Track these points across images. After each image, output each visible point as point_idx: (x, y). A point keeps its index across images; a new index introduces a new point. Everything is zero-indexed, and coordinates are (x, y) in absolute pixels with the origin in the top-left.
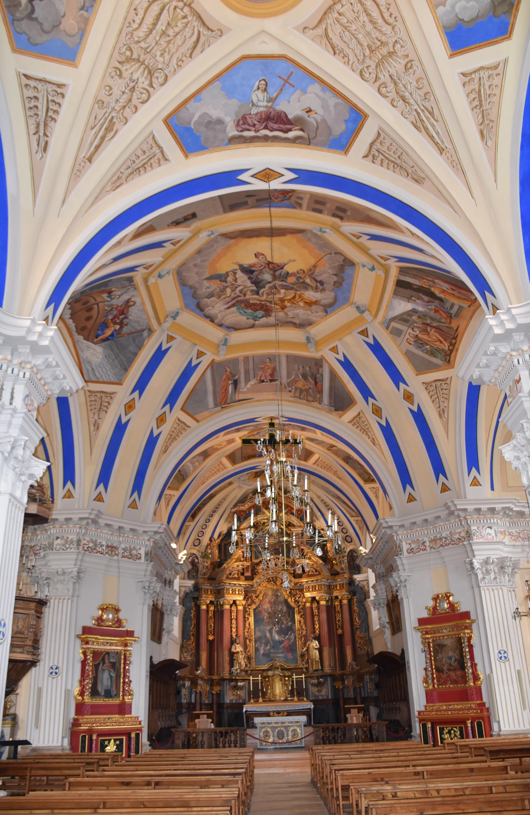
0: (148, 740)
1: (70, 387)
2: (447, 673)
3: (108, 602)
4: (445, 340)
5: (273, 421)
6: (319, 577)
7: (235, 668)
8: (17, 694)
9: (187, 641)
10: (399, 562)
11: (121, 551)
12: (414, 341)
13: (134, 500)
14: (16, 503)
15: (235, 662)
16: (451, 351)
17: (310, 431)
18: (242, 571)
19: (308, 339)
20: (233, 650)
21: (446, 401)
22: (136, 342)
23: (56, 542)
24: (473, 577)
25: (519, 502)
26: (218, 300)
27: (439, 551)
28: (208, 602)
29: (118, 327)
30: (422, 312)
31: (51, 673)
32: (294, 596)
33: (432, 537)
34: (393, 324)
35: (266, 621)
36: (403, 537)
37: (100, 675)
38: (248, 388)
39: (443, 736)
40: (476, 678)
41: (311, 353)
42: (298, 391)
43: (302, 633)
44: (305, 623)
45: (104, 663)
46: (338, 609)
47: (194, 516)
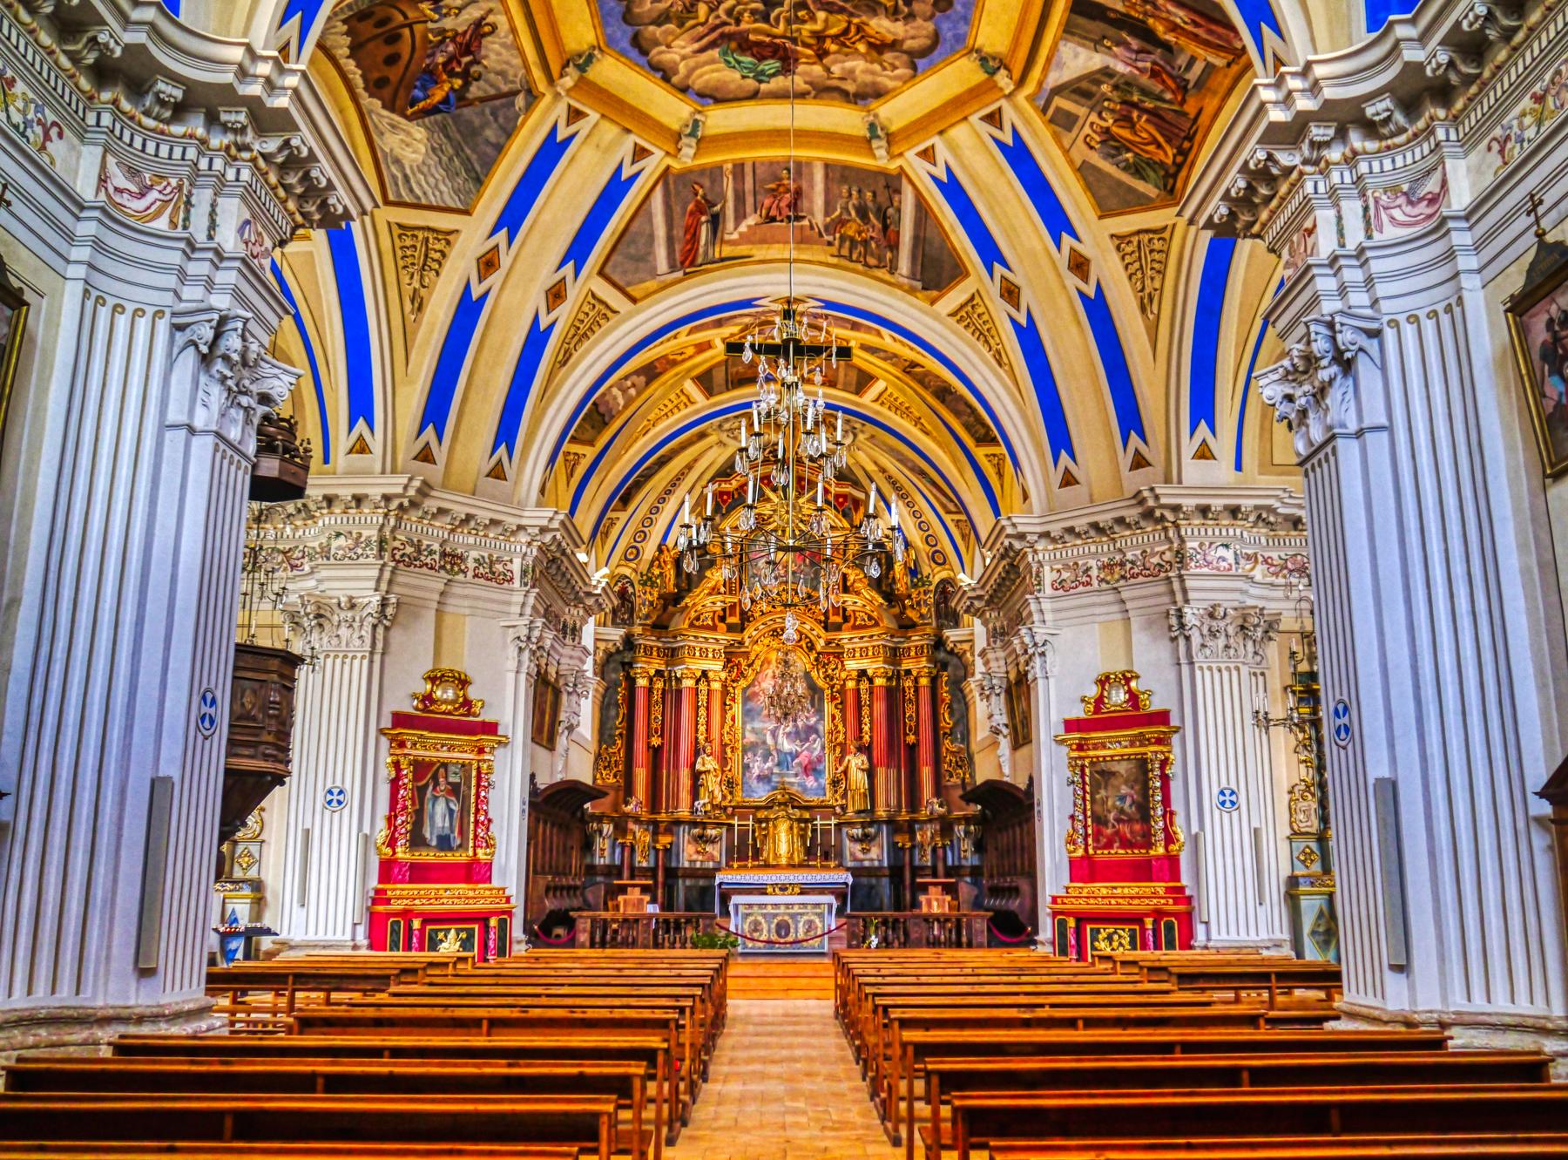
0: (525, 931)
1: (345, 208)
2: (1114, 826)
3: (446, 665)
4: (1169, 141)
5: (794, 307)
6: (875, 631)
7: (702, 802)
8: (263, 842)
9: (609, 746)
10: (1033, 607)
11: (471, 564)
12: (1102, 142)
13: (500, 461)
14: (229, 452)
15: (702, 790)
16: (1179, 167)
17: (869, 330)
18: (721, 614)
19: (872, 127)
20: (698, 767)
21: (1158, 278)
22: (501, 120)
23: (335, 544)
24: (1182, 641)
25: (1291, 497)
26: (678, 31)
27: (1115, 589)
28: (652, 672)
29: (458, 83)
30: (1123, 75)
31: (330, 802)
33: (1106, 560)
34: (1059, 102)
36: (1047, 557)
37: (428, 806)
38: (741, 234)
39: (1096, 944)
40: (1170, 839)
41: (880, 160)
42: (847, 244)
44: (844, 720)
45: (436, 784)
46: (910, 694)
47: (626, 500)
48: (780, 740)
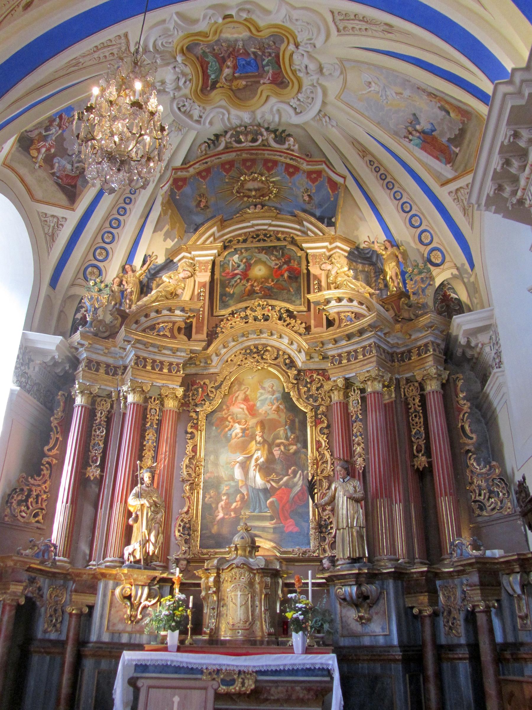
32: (306, 386)
35: (233, 441)
43: (322, 472)
48: (251, 473)
